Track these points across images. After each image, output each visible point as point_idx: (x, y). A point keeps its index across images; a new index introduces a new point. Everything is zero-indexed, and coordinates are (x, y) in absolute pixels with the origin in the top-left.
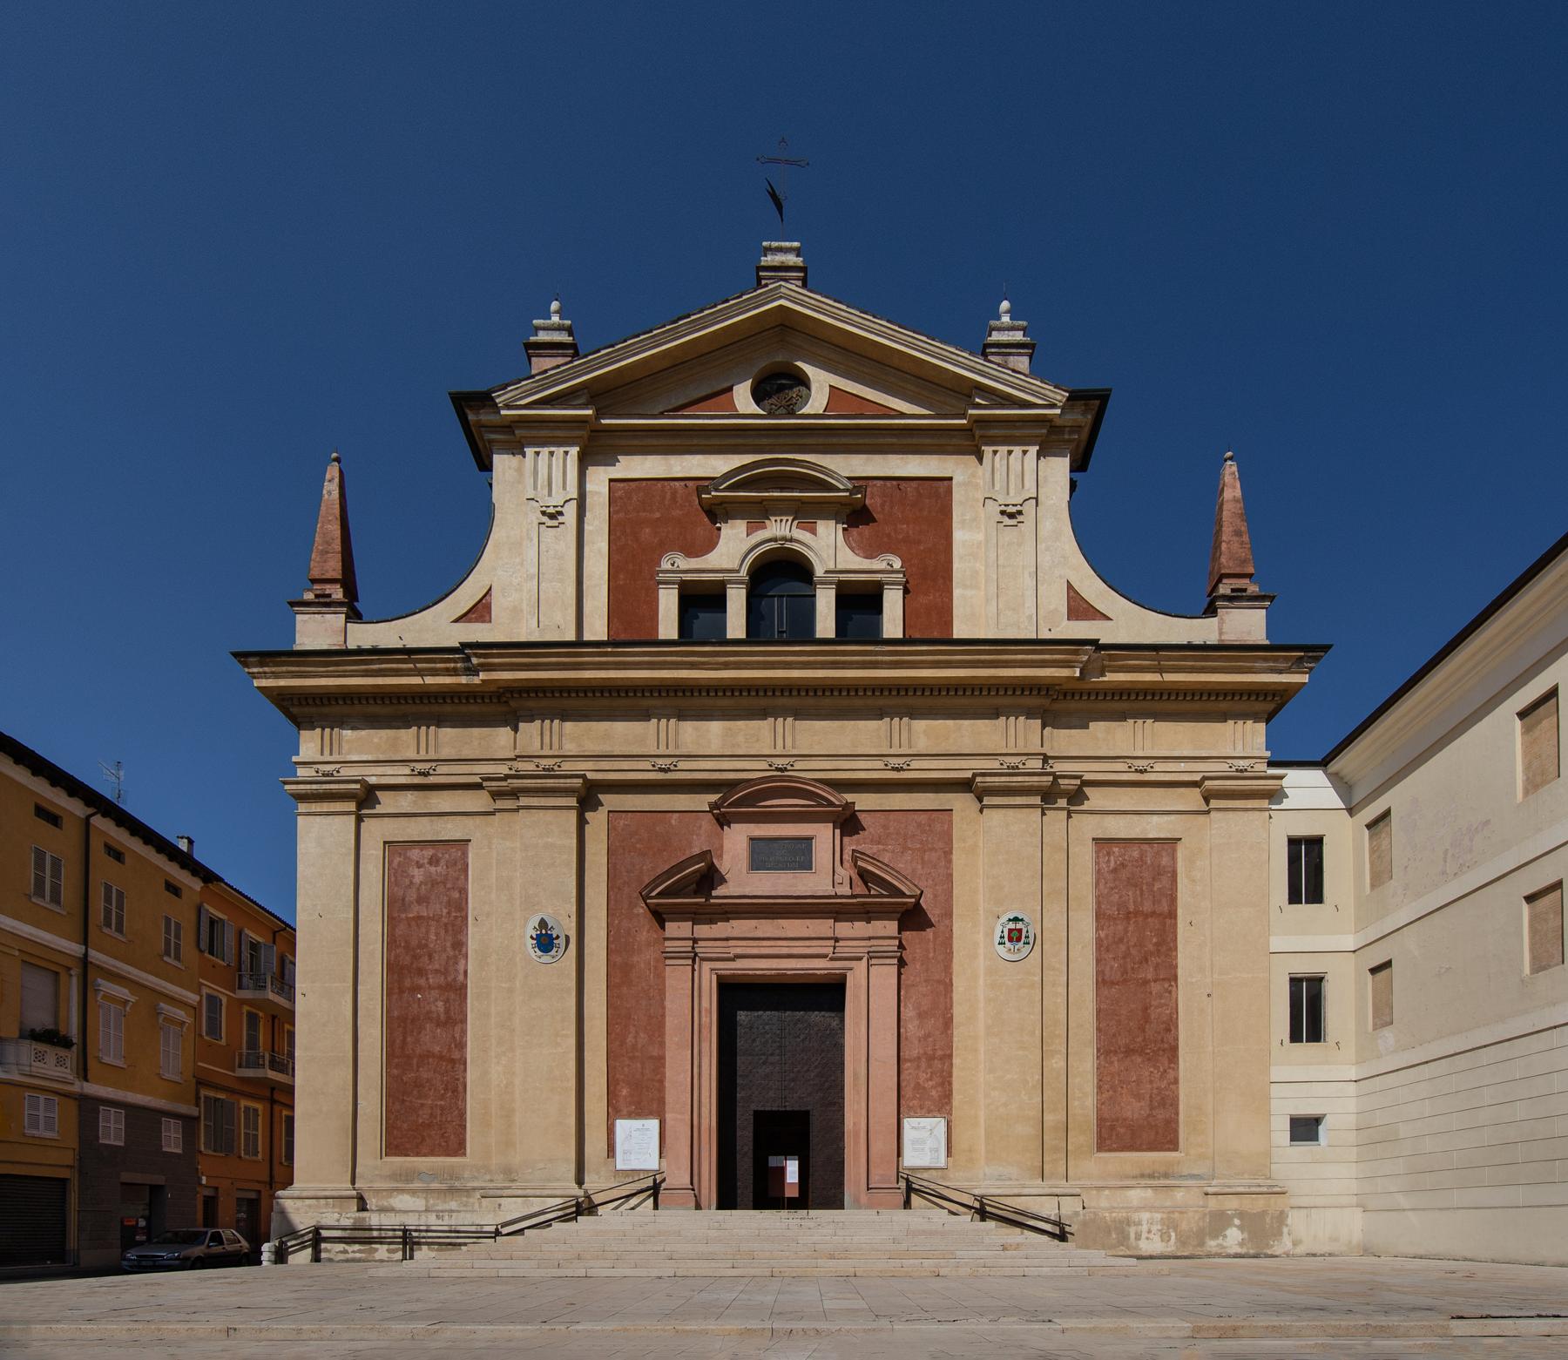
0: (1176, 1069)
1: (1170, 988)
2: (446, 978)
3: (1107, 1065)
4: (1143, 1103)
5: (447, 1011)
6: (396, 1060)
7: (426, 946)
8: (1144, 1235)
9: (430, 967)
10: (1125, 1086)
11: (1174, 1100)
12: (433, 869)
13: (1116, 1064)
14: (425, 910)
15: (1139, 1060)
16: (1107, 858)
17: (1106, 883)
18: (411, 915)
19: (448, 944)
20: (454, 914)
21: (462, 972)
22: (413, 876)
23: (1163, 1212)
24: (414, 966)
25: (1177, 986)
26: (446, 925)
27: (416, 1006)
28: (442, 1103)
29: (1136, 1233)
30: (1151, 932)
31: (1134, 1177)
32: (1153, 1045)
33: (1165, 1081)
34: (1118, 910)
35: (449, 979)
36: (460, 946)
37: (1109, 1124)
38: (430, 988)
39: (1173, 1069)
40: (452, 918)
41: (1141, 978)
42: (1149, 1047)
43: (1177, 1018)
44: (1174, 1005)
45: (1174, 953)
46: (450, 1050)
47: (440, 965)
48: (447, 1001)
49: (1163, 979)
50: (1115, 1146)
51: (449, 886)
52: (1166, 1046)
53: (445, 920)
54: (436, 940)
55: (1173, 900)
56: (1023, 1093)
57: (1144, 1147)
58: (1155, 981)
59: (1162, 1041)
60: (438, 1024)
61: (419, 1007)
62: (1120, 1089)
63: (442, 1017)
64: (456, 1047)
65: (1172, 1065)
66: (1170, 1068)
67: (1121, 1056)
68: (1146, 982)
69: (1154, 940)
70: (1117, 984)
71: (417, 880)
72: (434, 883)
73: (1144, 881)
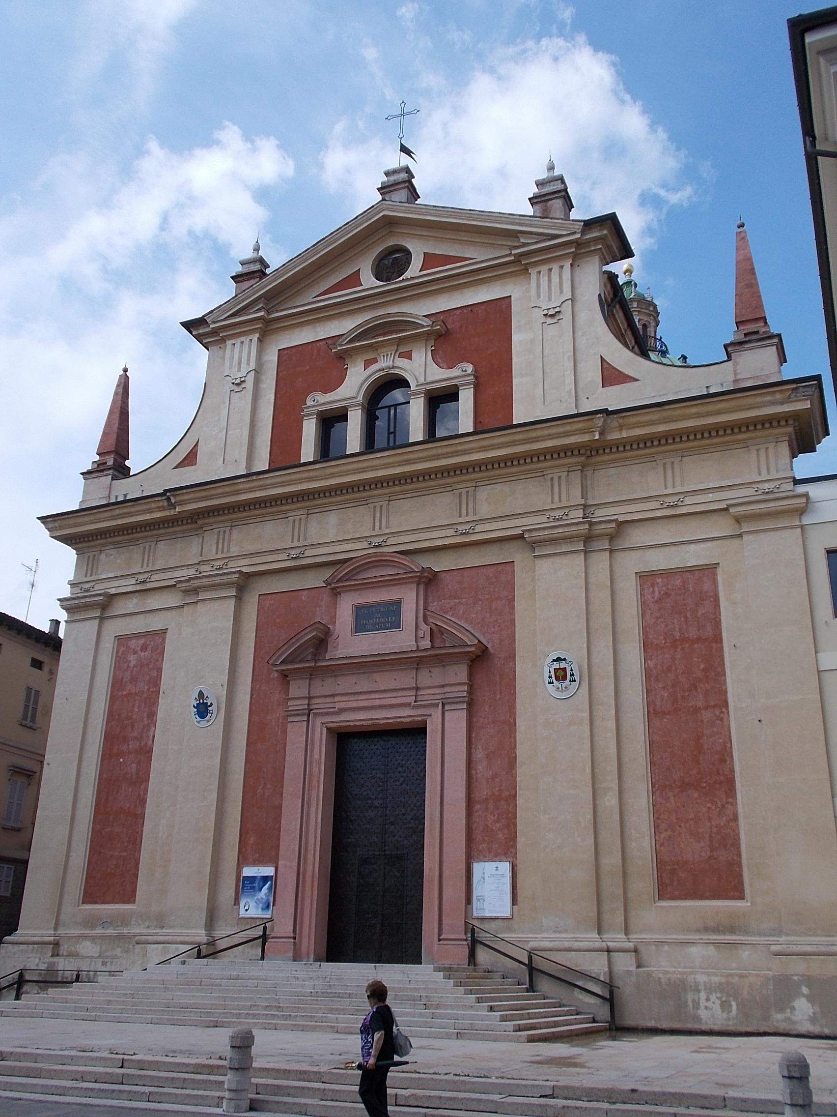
0: (734, 804)
1: (722, 715)
2: (140, 743)
3: (663, 801)
4: (702, 844)
5: (138, 770)
9: (131, 735)
10: (683, 825)
11: (735, 839)
12: (143, 654)
13: (672, 800)
14: (134, 687)
15: (696, 795)
16: (651, 589)
17: (652, 614)
18: (125, 693)
19: (145, 715)
20: (151, 690)
21: (151, 737)
22: (130, 662)
25: (728, 713)
30: (698, 659)
31: (698, 931)
32: (709, 778)
33: (724, 818)
34: (665, 639)
35: (143, 744)
36: (152, 715)
37: (668, 868)
39: (732, 804)
41: (691, 707)
42: (704, 780)
44: (727, 733)
45: (723, 678)
48: (139, 763)
49: (715, 706)
51: (151, 667)
52: (722, 778)
53: (145, 695)
54: (138, 712)
55: (717, 623)
56: (576, 835)
57: (708, 894)
58: (706, 708)
59: (718, 773)
62: (678, 827)
64: (139, 803)
65: (730, 800)
66: (728, 803)
67: (676, 791)
68: (696, 710)
69: (702, 666)
70: (668, 714)
71: (132, 665)
73: (688, 609)
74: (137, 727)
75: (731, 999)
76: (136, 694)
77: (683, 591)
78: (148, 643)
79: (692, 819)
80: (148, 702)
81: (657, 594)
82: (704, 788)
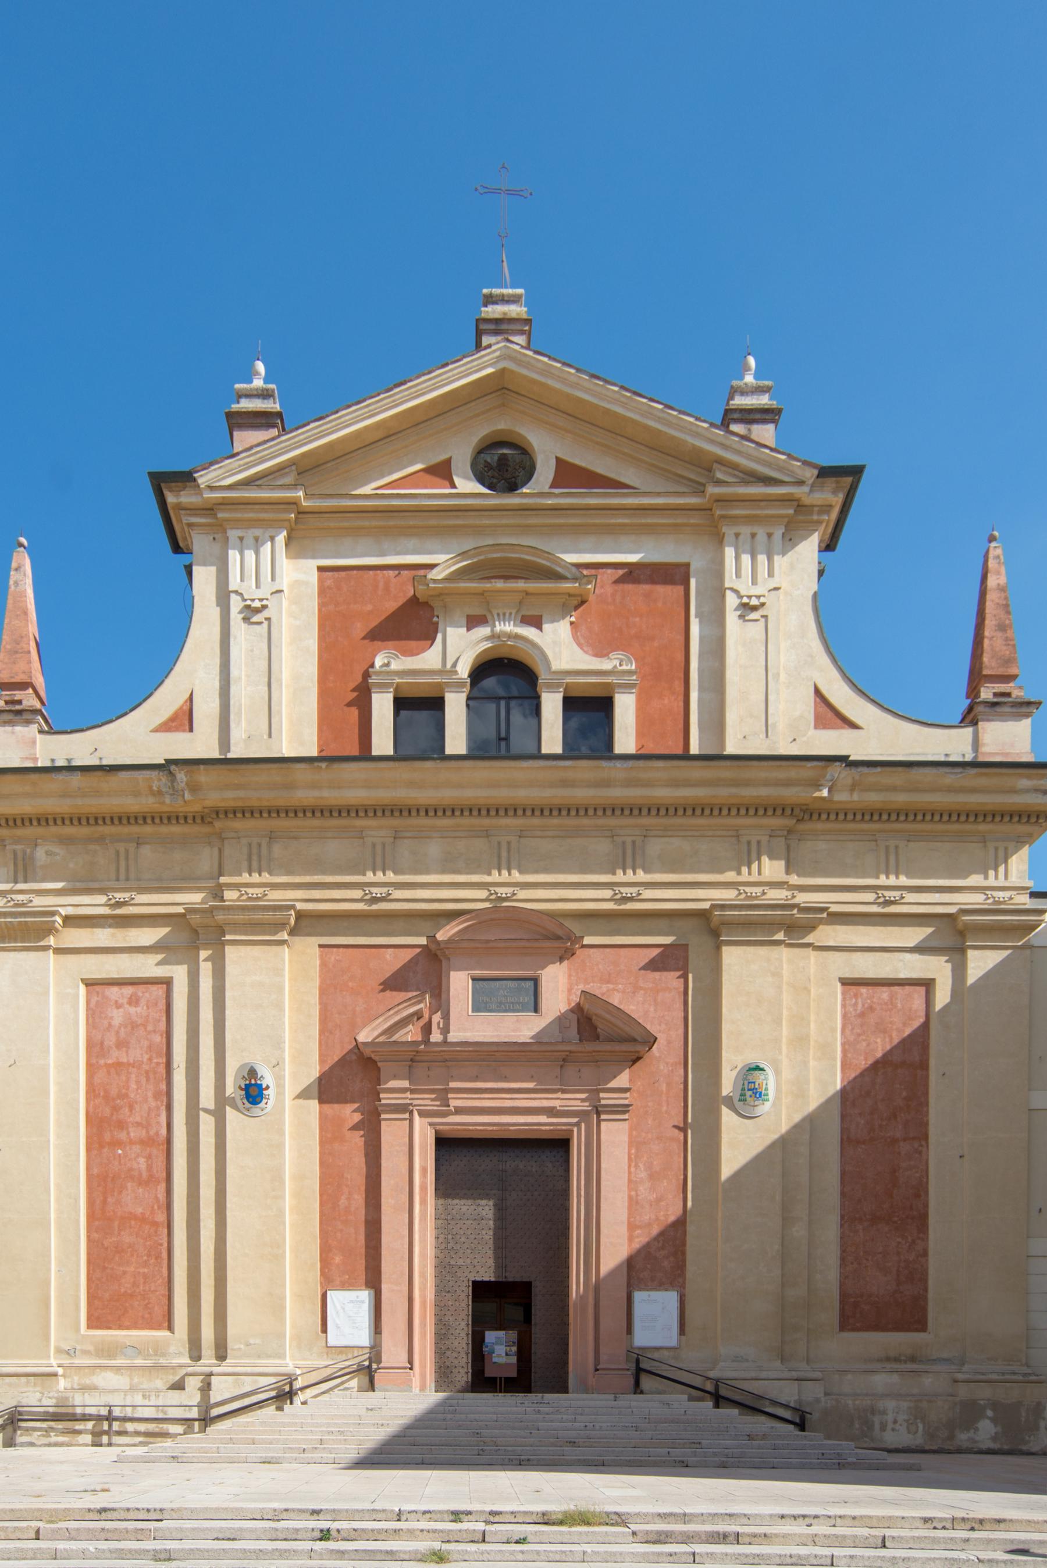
0: (926, 1239)
1: (920, 1148)
2: (147, 1132)
5: (149, 1168)
6: (97, 1223)
7: (126, 1095)
8: (890, 1426)
14: (124, 1054)
16: (854, 1000)
17: (853, 1029)
18: (110, 1061)
19: (150, 1094)
20: (155, 1061)
23: (910, 1401)
24: (114, 1118)
25: (928, 1146)
26: (147, 1072)
27: (116, 1163)
28: (146, 1270)
29: (881, 1423)
31: (879, 1360)
35: (152, 1133)
38: (132, 1142)
40: (153, 1065)
43: (927, 1183)
45: (925, 1109)
46: (153, 1212)
47: (141, 1117)
48: (149, 1157)
49: (914, 1138)
50: (858, 1325)
51: (150, 1028)
52: (915, 1213)
53: (145, 1067)
58: (905, 1140)
60: (141, 1182)
61: (120, 1164)
62: (865, 1261)
63: (145, 1174)
65: (921, 1235)
68: (894, 1141)
69: (904, 1094)
71: (117, 1021)
72: (134, 1026)
74: (138, 1109)
75: (918, 1421)
76: (129, 1064)
77: (890, 1007)
78: (140, 994)
79: (880, 1253)
80: (151, 1076)
81: (860, 1005)
82: (895, 1222)
